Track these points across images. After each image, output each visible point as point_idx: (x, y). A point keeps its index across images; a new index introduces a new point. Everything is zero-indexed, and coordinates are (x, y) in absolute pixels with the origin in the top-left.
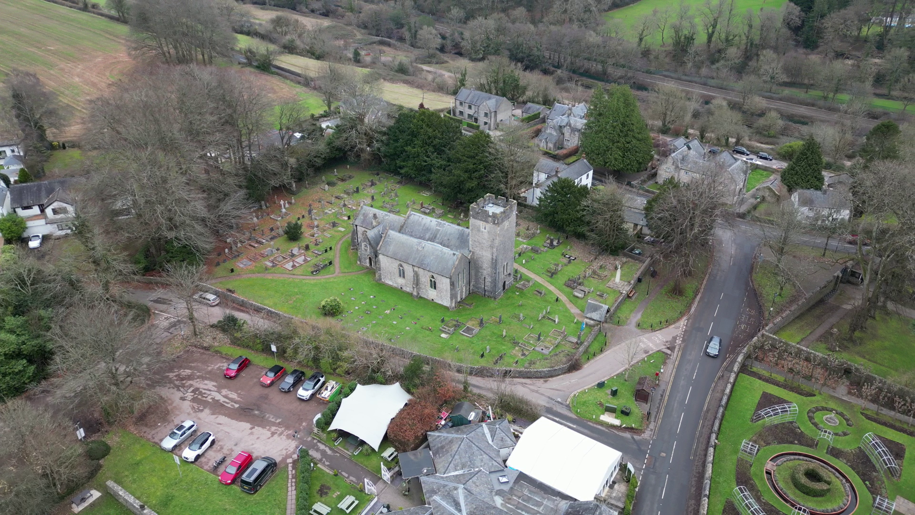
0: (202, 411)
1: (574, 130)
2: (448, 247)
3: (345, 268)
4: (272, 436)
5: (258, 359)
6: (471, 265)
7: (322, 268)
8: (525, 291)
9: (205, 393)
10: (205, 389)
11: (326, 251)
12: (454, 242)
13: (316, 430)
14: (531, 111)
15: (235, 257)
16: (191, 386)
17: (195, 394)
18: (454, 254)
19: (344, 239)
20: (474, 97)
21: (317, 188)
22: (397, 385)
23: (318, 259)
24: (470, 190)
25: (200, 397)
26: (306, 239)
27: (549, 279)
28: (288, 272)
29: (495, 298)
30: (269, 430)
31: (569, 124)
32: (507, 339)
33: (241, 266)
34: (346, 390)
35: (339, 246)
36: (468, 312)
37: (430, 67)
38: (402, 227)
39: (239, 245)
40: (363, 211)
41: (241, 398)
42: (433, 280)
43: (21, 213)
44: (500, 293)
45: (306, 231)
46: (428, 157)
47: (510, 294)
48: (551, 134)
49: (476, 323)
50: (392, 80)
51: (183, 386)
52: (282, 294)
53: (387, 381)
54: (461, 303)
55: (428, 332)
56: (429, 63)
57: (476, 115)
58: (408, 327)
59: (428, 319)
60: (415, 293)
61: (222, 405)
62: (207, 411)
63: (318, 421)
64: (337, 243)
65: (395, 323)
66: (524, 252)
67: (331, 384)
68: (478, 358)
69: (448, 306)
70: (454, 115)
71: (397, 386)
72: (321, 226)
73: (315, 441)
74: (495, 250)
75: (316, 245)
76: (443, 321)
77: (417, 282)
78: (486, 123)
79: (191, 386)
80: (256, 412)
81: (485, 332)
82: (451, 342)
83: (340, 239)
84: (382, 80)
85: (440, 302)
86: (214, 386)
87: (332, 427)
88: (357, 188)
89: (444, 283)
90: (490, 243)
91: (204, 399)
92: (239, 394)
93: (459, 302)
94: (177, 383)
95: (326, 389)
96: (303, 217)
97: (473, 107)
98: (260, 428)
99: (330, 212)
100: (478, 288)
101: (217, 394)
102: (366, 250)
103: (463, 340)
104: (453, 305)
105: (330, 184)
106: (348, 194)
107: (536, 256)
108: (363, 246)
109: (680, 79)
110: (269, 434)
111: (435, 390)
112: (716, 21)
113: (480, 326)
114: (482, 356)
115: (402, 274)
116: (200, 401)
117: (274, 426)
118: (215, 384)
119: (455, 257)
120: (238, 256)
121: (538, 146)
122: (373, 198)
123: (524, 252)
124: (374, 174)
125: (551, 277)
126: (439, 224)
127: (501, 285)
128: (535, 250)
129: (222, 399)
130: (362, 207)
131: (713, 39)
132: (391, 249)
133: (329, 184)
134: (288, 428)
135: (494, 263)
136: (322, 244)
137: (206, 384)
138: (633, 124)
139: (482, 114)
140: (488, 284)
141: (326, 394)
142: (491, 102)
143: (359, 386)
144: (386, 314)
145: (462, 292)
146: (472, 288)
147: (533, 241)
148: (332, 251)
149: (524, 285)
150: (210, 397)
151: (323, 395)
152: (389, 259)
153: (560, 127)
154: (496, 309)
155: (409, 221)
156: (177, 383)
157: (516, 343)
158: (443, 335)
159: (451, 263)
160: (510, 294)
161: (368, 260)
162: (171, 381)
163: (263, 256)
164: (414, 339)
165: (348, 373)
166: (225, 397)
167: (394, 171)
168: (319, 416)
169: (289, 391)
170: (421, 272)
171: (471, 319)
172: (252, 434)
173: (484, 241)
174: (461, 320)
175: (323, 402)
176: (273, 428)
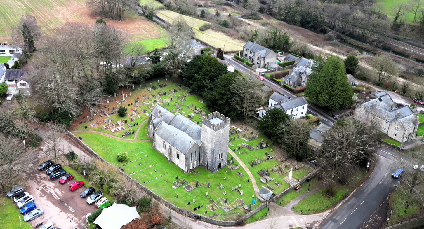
0: (43, 197)
2: (191, 136)
3: (140, 137)
4: (68, 218)
5: (78, 178)
6: (201, 149)
7: (128, 134)
8: (232, 171)
9: (48, 189)
10: (48, 187)
11: (134, 125)
12: (195, 134)
13: (87, 221)
15: (90, 120)
16: (44, 183)
17: (44, 188)
18: (191, 142)
19: (146, 121)
21: (145, 89)
22: (135, 208)
23: (129, 129)
24: (222, 105)
25: (45, 190)
26: (127, 118)
27: (250, 167)
28: (111, 133)
29: (212, 172)
30: (67, 215)
32: (208, 197)
33: (91, 126)
34: (110, 204)
35: (142, 124)
36: (194, 177)
37: (251, 21)
38: (172, 120)
39: (95, 114)
40: (156, 108)
41: (62, 195)
42: (178, 154)
43: (8, 83)
44: (216, 169)
45: (129, 112)
47: (223, 171)
49: (195, 184)
50: (217, 30)
51: (40, 183)
52: (104, 145)
53: (131, 205)
54: (192, 171)
55: (166, 183)
58: (157, 177)
59: (170, 175)
60: (169, 159)
61: (53, 197)
62: (45, 198)
63: (89, 217)
64: (142, 122)
65: (151, 173)
66: (243, 148)
67: (104, 199)
68: (186, 204)
69: (184, 170)
70: (242, 56)
71: (135, 208)
72: (138, 111)
73: (85, 227)
74: (213, 144)
75: (132, 121)
76: (177, 178)
77: (170, 153)
79: (44, 183)
80: (66, 204)
81: (198, 191)
82: (176, 192)
83: (144, 120)
84: (211, 29)
86: (53, 186)
87: (94, 223)
88: (165, 93)
89: (183, 157)
90: (211, 140)
91: (46, 191)
92: (62, 193)
93: (191, 169)
94: (38, 180)
95: (101, 201)
96: (132, 104)
97: (252, 53)
98: (64, 213)
99: (146, 104)
100: (204, 164)
101: (53, 190)
102: (152, 129)
103: (183, 192)
104: (186, 170)
105: (153, 88)
106: (160, 95)
107: (248, 151)
108: (151, 127)
110: (66, 217)
111: (150, 216)
113: (196, 186)
114: (189, 203)
115: (165, 147)
116: (44, 192)
117: (70, 213)
118: (54, 185)
119: (191, 144)
120: (92, 120)
121: (284, 83)
122: (171, 99)
123: (243, 148)
124: (178, 86)
125: (252, 166)
126: (190, 123)
127: (217, 165)
128: (249, 148)
129: (53, 193)
130: (156, 105)
132: (161, 131)
133: (152, 88)
134: (76, 216)
135: (213, 152)
136: (134, 121)
137: (50, 184)
138: (337, 80)
139: (256, 58)
140: (209, 162)
141: (99, 204)
142: (263, 52)
143: (115, 204)
144: (149, 167)
145: (193, 164)
146: (201, 162)
147: (252, 142)
148: (138, 126)
149: (232, 168)
150: (49, 191)
151: (98, 204)
154: (210, 178)
155: (176, 118)
156: (38, 180)
157: (212, 201)
158: (174, 187)
159: (188, 146)
160: (223, 171)
161: (152, 135)
162: (36, 179)
163: (103, 122)
164: (157, 185)
165: (115, 195)
166: (56, 193)
167: (188, 85)
168: (90, 214)
169: (84, 197)
170: (173, 148)
171: (193, 181)
172: (59, 214)
173: (209, 138)
174: (187, 180)
175: (97, 207)
176: (70, 214)
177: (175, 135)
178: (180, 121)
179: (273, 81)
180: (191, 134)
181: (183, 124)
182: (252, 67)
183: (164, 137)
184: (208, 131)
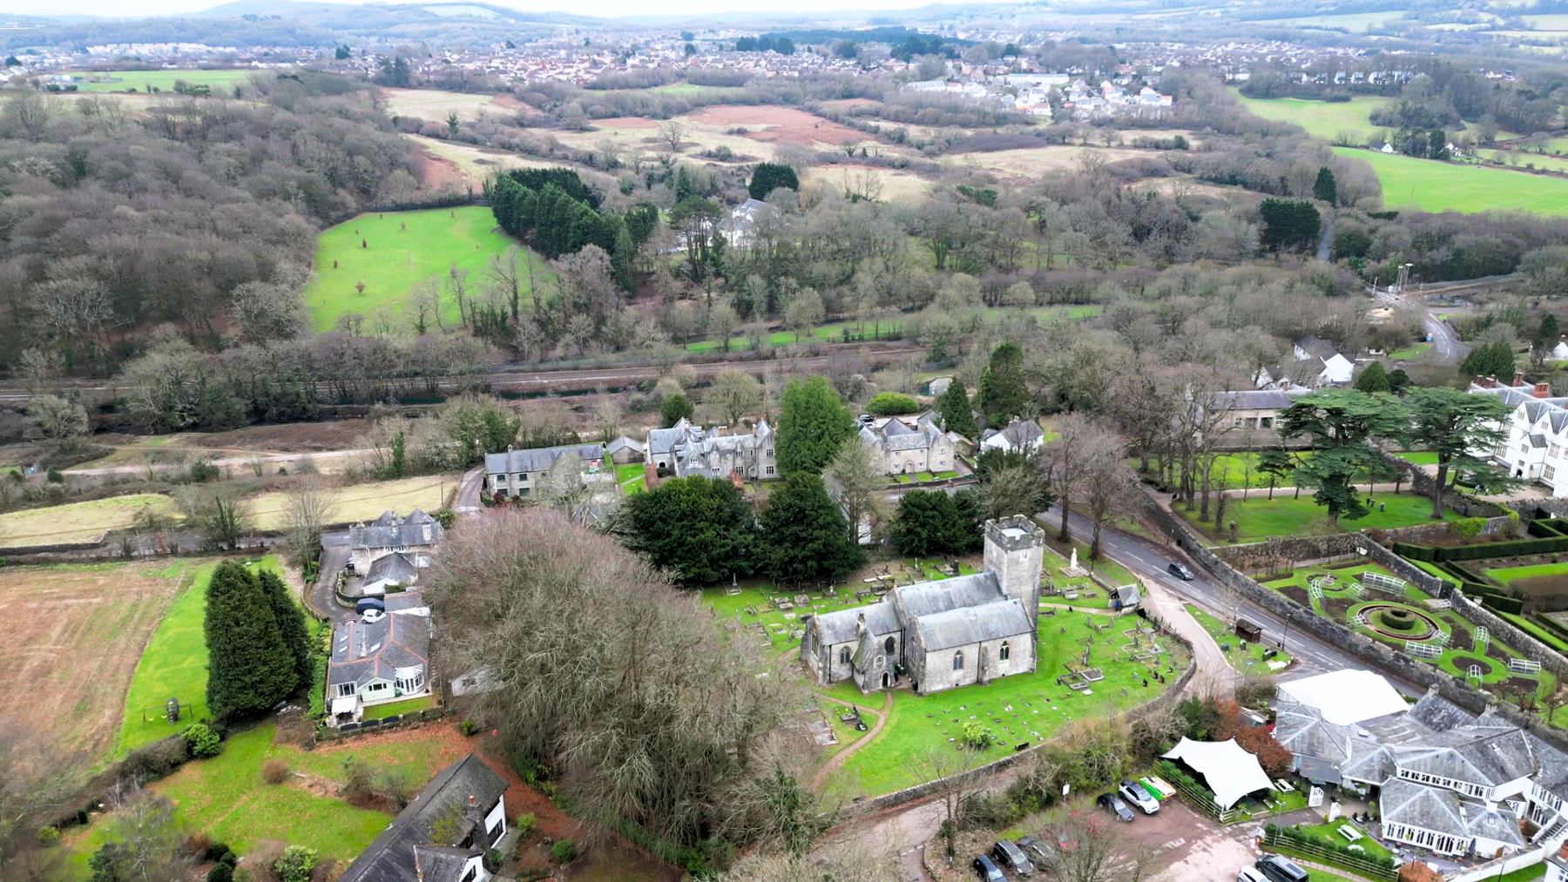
1: (723, 453)
2: (975, 605)
12: (977, 595)
14: (585, 453)
20: (521, 460)
31: (716, 448)
46: (725, 538)
56: (79, 462)
85: (1014, 672)
102: (880, 666)
109: (536, 371)
112: (514, 282)
126: (943, 586)
131: (519, 308)
152: (942, 653)
153: (703, 455)
159: (1020, 615)
161: (881, 681)
177: (973, 618)
178: (921, 598)
180: (968, 601)
181: (935, 599)
183: (956, 642)
184: (1022, 560)
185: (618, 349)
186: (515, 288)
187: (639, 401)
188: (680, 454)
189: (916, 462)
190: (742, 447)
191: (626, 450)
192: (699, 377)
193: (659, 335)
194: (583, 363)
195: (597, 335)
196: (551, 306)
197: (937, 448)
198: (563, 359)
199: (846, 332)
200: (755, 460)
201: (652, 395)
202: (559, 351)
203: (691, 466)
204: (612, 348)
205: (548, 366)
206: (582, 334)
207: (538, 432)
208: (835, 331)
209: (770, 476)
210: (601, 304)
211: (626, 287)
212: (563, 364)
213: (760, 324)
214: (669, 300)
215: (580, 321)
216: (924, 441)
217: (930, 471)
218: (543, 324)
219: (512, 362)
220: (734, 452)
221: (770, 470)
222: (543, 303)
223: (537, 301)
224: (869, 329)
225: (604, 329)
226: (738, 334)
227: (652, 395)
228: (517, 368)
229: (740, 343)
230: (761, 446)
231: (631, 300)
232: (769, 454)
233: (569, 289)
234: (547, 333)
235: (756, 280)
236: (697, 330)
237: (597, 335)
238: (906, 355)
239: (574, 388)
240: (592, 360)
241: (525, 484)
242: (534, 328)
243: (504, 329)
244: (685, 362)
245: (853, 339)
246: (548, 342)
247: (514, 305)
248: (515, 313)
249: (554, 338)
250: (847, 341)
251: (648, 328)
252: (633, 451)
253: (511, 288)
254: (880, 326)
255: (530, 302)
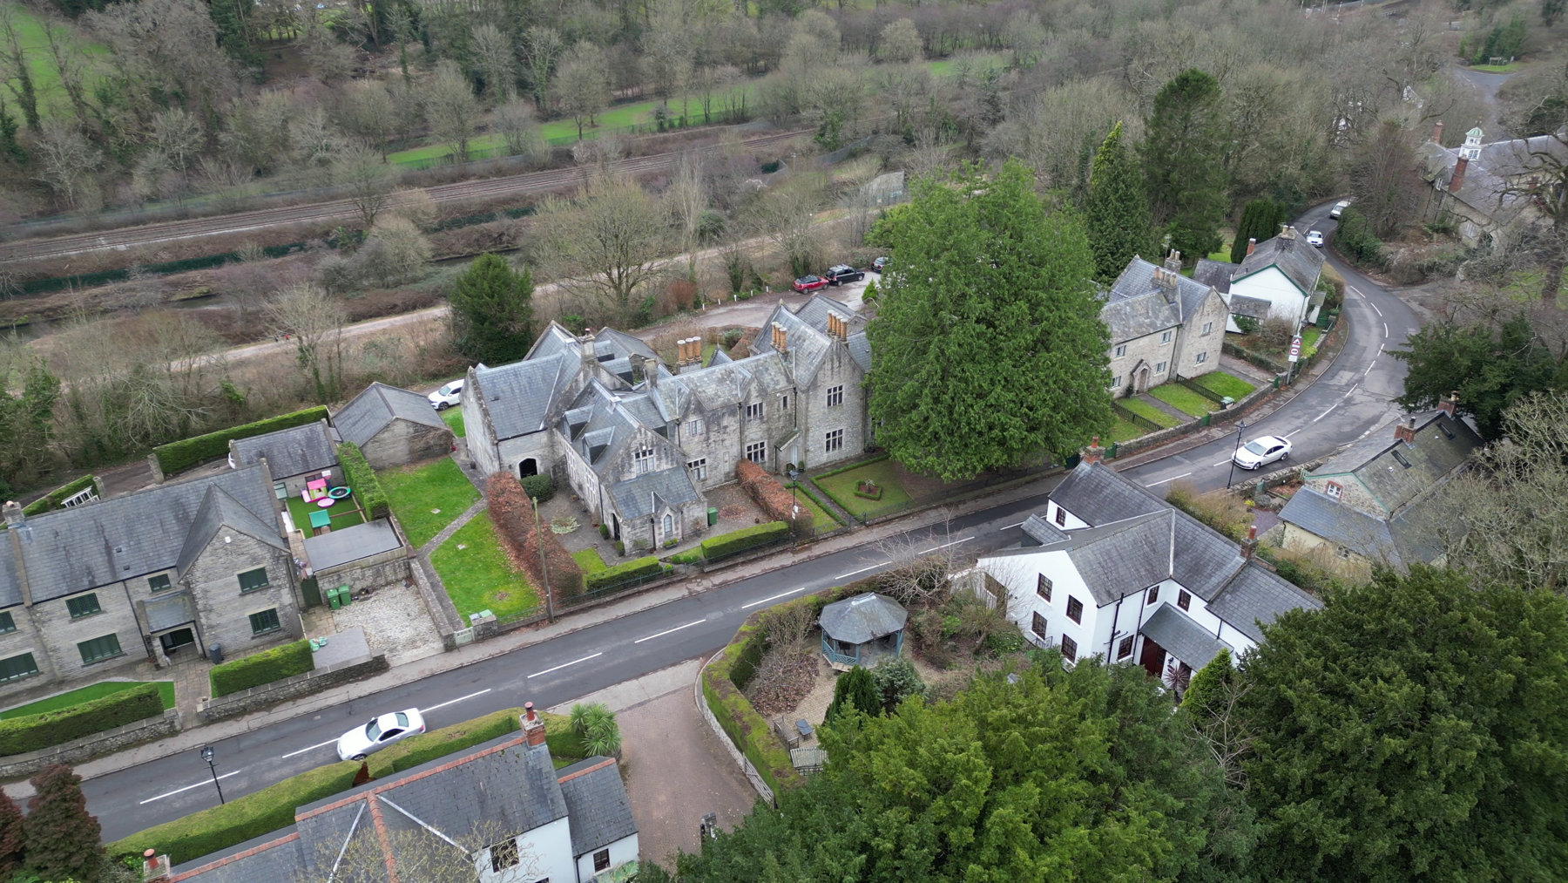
1: (712, 417)
14: (280, 459)
20: (62, 548)
31: (695, 406)
48: (647, 477)
57: (166, 619)
78: (264, 621)
112: (18, 58)
131: (41, 109)
153: (662, 431)
179: (606, 593)
182: (311, 667)
185: (258, 173)
186: (23, 69)
187: (339, 271)
188: (593, 436)
189: (1153, 364)
190: (763, 392)
191: (401, 429)
192: (440, 209)
193: (337, 141)
194: (192, 204)
195: (212, 147)
196: (105, 99)
197: (1198, 322)
198: (151, 199)
199: (659, 115)
200: (793, 425)
201: (362, 255)
202: (140, 185)
203: (636, 469)
204: (250, 169)
205: (124, 215)
206: (181, 148)
207: (117, 401)
208: (639, 116)
209: (835, 455)
210: (207, 91)
211: (247, 61)
212: (152, 209)
213: (517, 108)
214: (332, 78)
215: (170, 120)
216: (1165, 311)
217: (1179, 381)
218: (95, 137)
219: (41, 214)
220: (745, 410)
221: (833, 441)
222: (89, 96)
223: (75, 91)
224: (695, 108)
225: (223, 137)
226: (481, 129)
227: (362, 255)
228: (55, 225)
229: (490, 145)
230: (814, 385)
231: (262, 80)
232: (835, 398)
233: (136, 66)
234: (107, 153)
235: (488, 35)
236: (400, 131)
237: (212, 147)
238: (787, 142)
239: (188, 255)
240: (213, 197)
241: (93, 628)
242: (77, 143)
243: (14, 151)
244: (409, 182)
245: (672, 126)
246: (114, 168)
247: (29, 105)
248: (33, 119)
249: (125, 159)
250: (662, 129)
251: (310, 129)
252: (420, 430)
253: (12, 68)
254: (714, 101)
255: (64, 99)
